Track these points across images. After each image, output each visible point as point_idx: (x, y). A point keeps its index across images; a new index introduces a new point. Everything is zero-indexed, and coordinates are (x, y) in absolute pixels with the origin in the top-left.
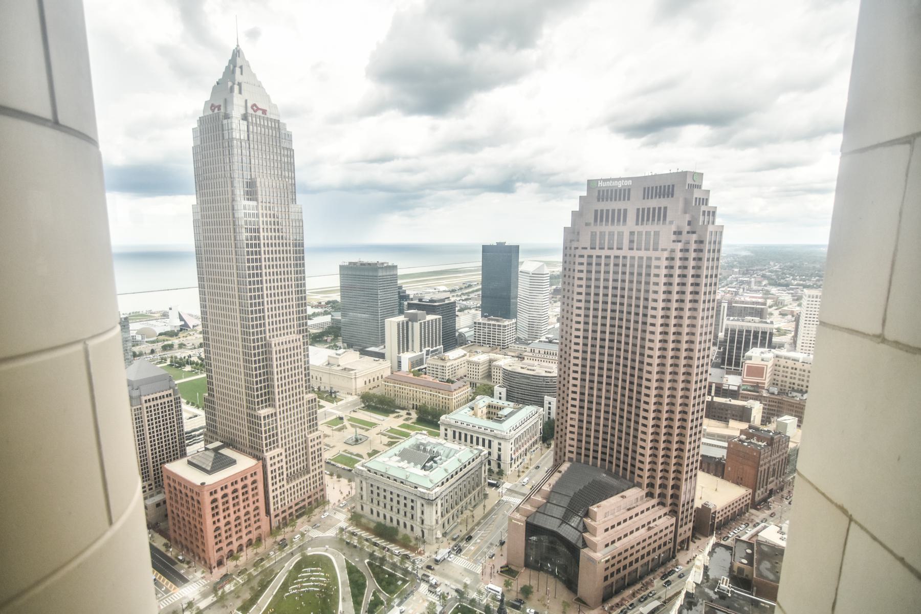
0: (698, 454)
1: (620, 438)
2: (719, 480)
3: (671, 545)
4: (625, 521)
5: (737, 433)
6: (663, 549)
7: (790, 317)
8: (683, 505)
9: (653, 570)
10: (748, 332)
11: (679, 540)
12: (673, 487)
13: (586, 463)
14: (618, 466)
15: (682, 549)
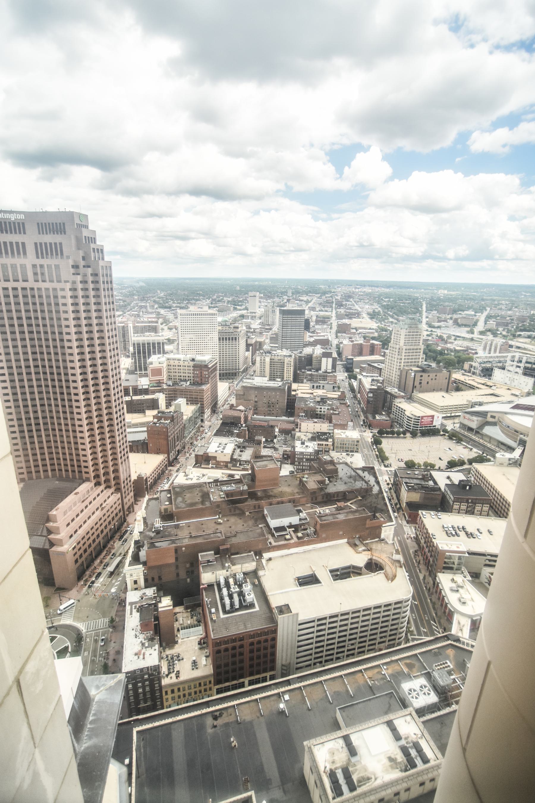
0: (126, 442)
1: (63, 448)
2: (146, 455)
3: (122, 513)
4: (82, 511)
5: (151, 419)
6: (116, 519)
7: (174, 330)
8: (124, 482)
9: (112, 537)
10: (149, 344)
11: (126, 507)
12: (113, 472)
13: (39, 477)
14: (67, 471)
15: (130, 512)
